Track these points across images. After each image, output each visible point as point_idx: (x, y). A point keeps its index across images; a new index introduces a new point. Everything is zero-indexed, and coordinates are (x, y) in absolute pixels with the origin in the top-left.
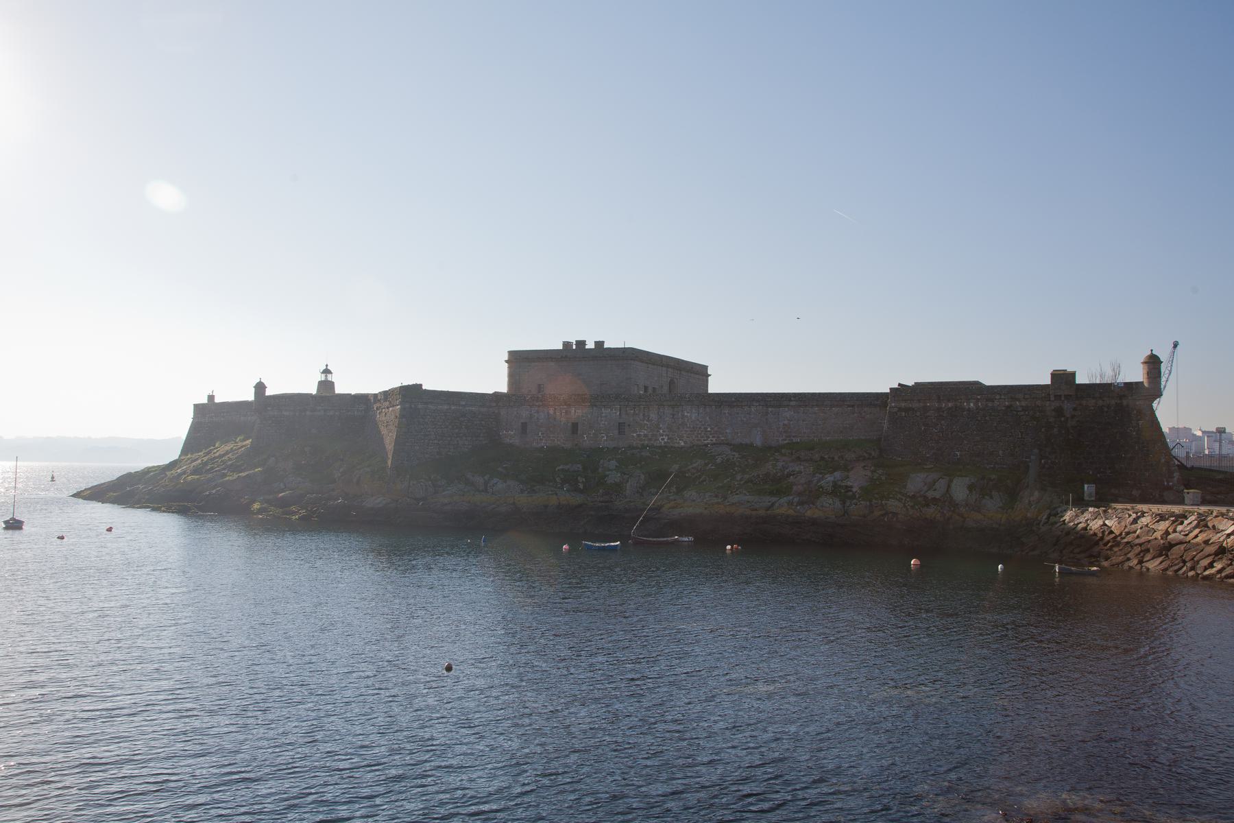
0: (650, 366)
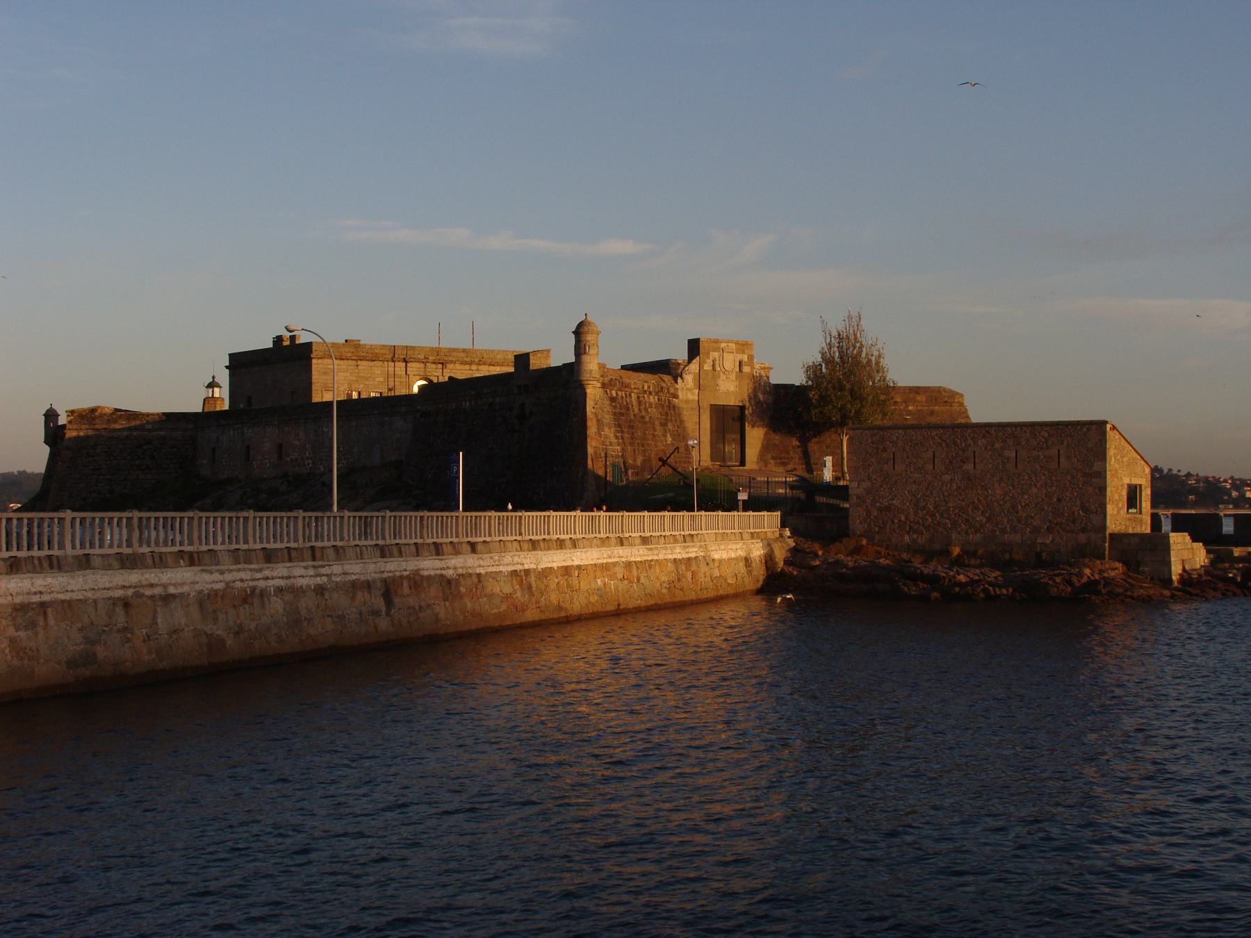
0: (359, 362)
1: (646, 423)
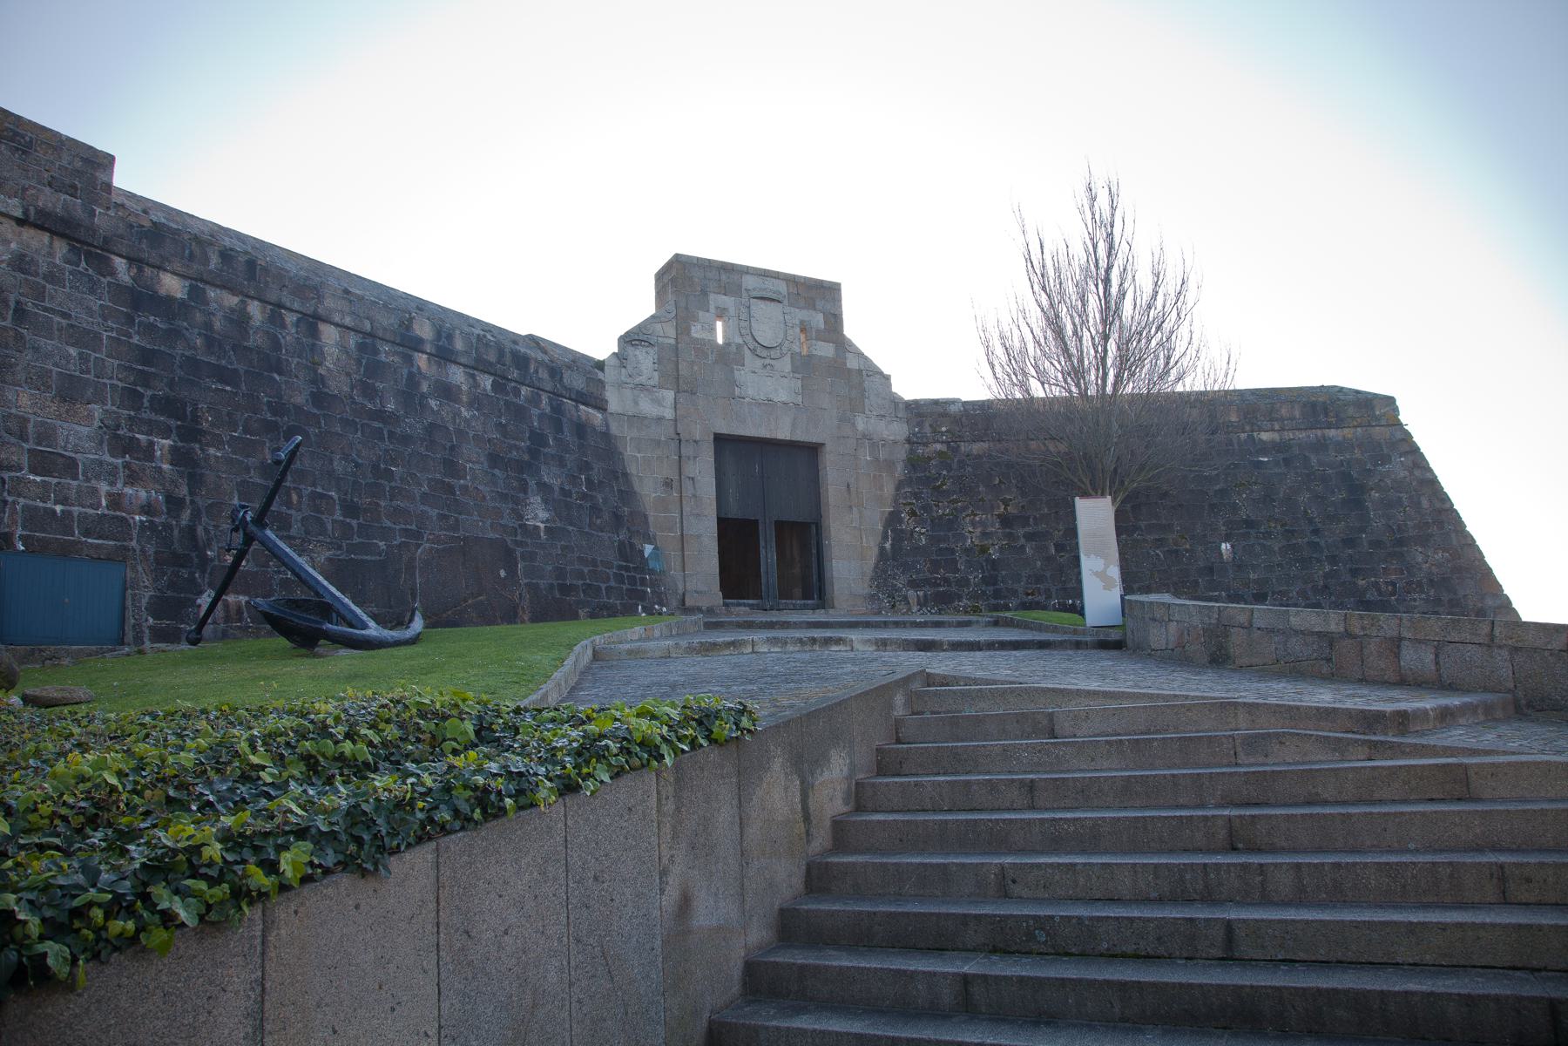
1: (406, 439)
